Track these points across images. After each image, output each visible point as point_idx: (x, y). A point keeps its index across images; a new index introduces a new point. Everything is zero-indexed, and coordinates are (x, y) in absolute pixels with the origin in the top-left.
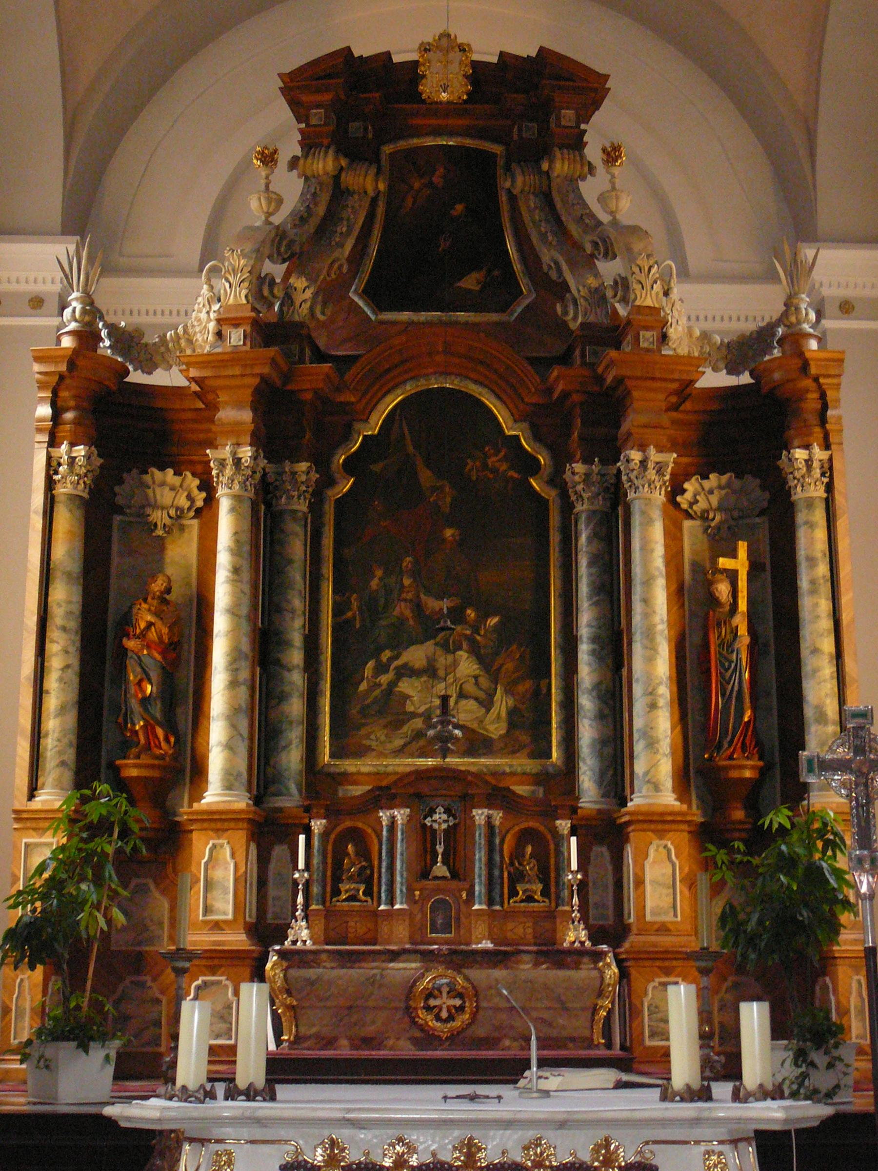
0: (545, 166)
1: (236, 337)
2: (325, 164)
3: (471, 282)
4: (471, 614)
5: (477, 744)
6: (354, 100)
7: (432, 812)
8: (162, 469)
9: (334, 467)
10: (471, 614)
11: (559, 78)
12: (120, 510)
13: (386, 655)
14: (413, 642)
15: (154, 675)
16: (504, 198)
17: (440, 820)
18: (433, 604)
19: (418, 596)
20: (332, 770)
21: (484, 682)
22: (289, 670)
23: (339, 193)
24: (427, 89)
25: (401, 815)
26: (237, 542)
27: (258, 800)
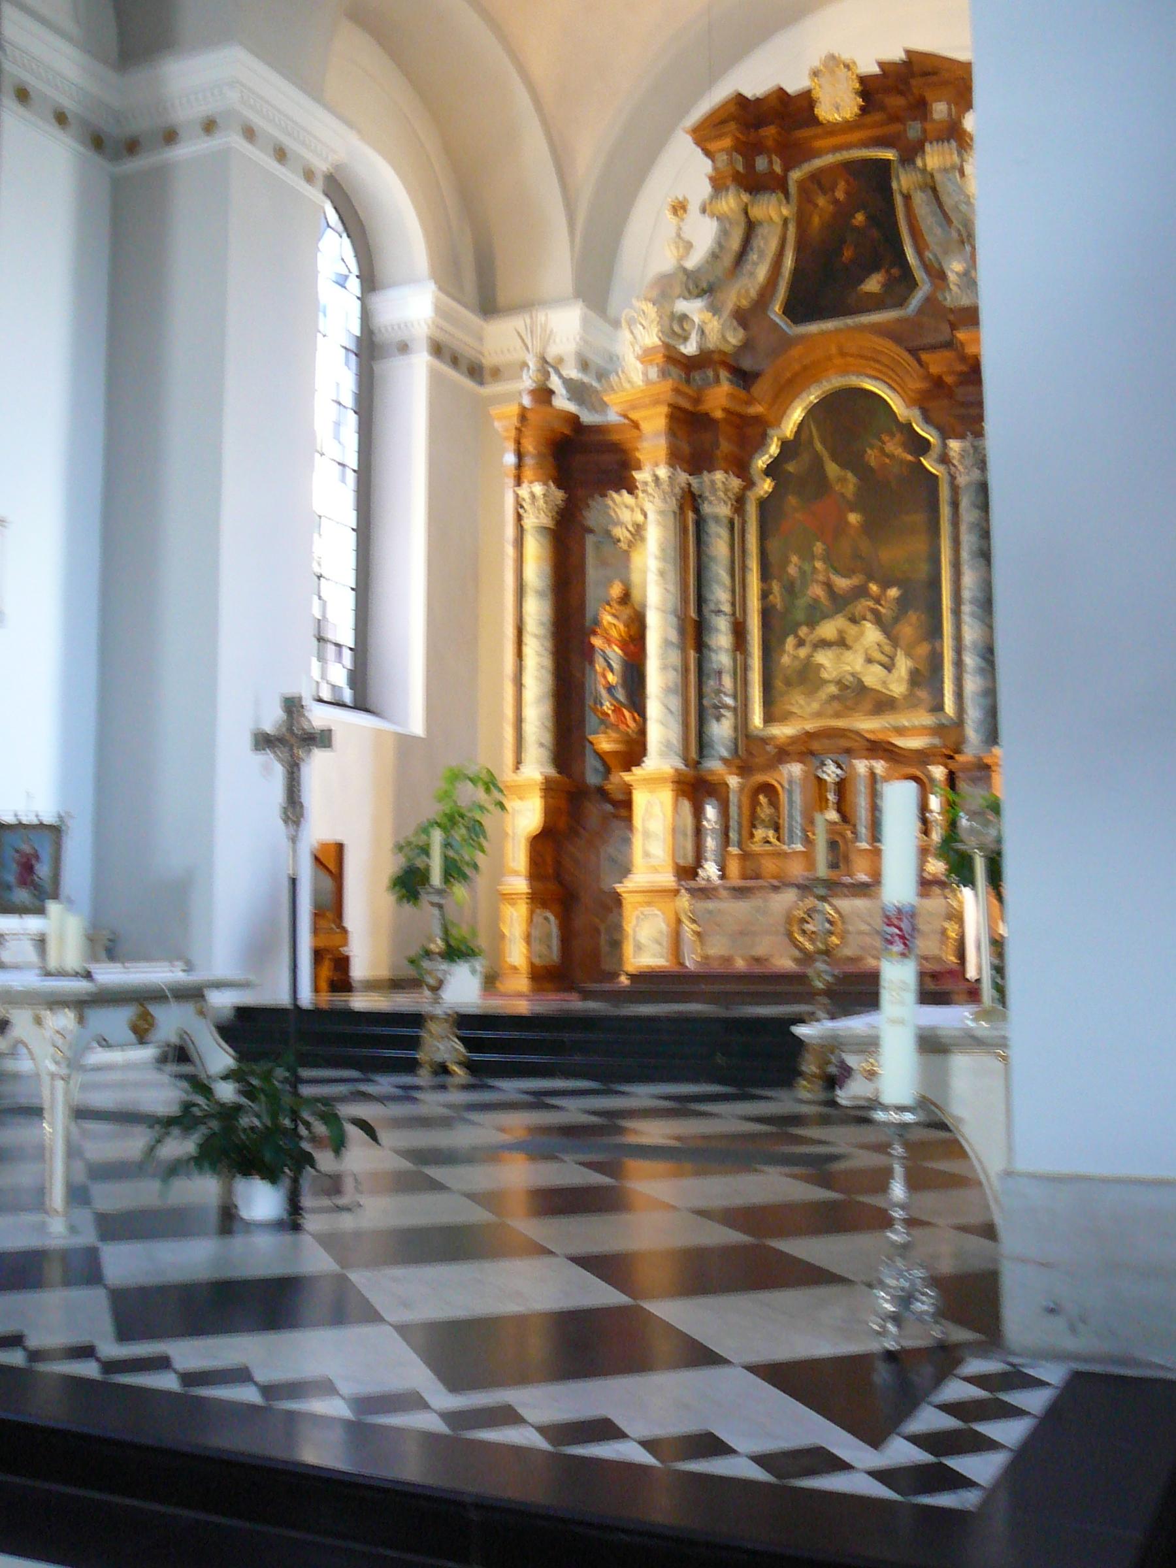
0: (919, 163)
2: (730, 202)
3: (873, 284)
4: (874, 588)
5: (884, 704)
7: (823, 764)
8: (617, 491)
9: (752, 471)
10: (874, 588)
11: (926, 74)
12: (591, 531)
13: (803, 631)
14: (825, 616)
15: (616, 666)
16: (899, 201)
18: (842, 583)
19: (829, 578)
20: (762, 734)
21: (888, 649)
22: (715, 652)
24: (826, 112)
25: (795, 769)
26: (663, 550)
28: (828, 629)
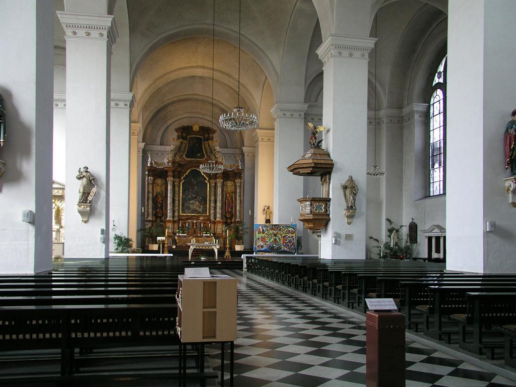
1: (170, 164)
2: (181, 140)
3: (199, 155)
6: (185, 131)
17: (195, 221)
23: (182, 142)
24: (194, 129)
25: (190, 221)
27: (173, 219)
28: (191, 202)
